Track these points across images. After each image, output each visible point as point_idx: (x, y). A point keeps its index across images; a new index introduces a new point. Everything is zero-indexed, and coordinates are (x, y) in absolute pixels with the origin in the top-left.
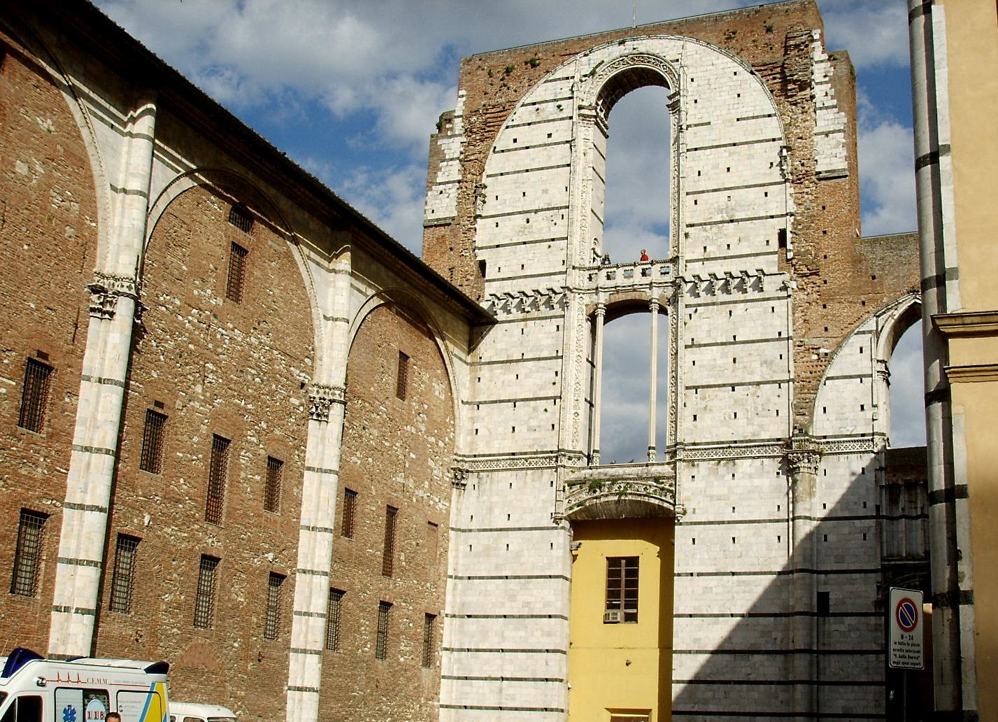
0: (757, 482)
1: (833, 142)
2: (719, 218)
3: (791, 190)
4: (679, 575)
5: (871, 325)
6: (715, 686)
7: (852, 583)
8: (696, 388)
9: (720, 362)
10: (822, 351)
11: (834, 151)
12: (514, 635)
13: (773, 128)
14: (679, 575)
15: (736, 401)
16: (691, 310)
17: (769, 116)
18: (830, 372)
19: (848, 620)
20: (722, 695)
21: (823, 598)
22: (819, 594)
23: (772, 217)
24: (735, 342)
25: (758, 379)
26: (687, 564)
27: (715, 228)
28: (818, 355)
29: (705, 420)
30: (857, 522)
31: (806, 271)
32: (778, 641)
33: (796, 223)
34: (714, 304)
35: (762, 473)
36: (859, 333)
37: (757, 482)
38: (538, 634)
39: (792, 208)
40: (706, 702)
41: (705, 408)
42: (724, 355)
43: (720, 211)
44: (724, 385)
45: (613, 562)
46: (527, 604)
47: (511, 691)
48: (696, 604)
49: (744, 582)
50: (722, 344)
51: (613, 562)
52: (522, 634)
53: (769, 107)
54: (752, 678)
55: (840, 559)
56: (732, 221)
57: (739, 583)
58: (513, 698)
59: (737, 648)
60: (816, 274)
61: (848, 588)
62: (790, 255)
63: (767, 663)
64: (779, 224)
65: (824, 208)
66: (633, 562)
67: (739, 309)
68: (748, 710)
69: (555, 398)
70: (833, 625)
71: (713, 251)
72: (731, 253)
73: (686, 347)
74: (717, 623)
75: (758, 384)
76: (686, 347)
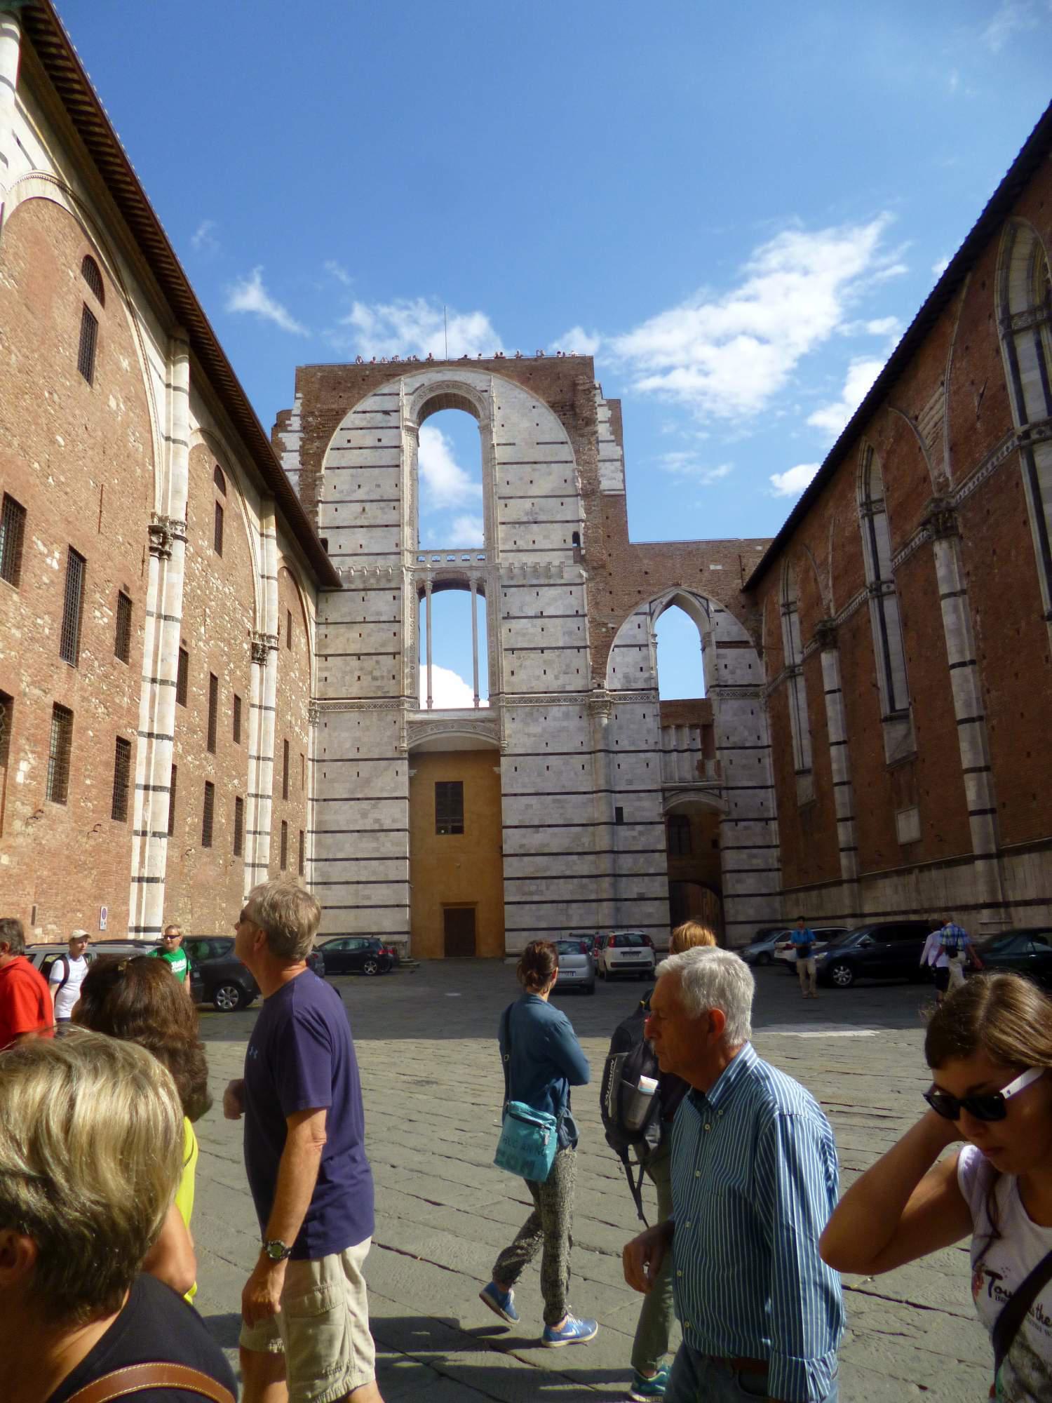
0: (565, 724)
1: (613, 468)
2: (525, 519)
3: (582, 502)
4: (505, 795)
5: (646, 608)
6: (539, 881)
7: (639, 799)
8: (513, 650)
9: (531, 630)
10: (610, 625)
11: (614, 475)
12: (367, 846)
13: (567, 452)
14: (505, 795)
15: (545, 661)
16: (505, 590)
17: (562, 443)
18: (616, 641)
19: (639, 828)
20: (544, 887)
21: (619, 811)
22: (617, 808)
23: (567, 522)
24: (541, 615)
25: (561, 644)
26: (512, 786)
27: (522, 527)
28: (607, 628)
29: (521, 675)
30: (641, 755)
31: (595, 564)
32: (587, 845)
33: (586, 527)
34: (523, 586)
35: (566, 716)
36: (636, 614)
37: (565, 724)
38: (388, 845)
39: (583, 515)
40: (531, 893)
41: (521, 666)
42: (534, 626)
43: (527, 514)
44: (535, 649)
45: (441, 787)
46: (377, 821)
47: (367, 892)
48: (520, 818)
49: (559, 801)
50: (531, 617)
51: (441, 787)
52: (375, 845)
53: (562, 435)
54: (568, 873)
55: (630, 782)
56: (536, 523)
57: (554, 801)
58: (368, 897)
59: (555, 851)
60: (603, 566)
61: (637, 804)
62: (583, 552)
63: (578, 862)
64: (571, 528)
65: (607, 518)
66: (457, 787)
67: (544, 591)
68: (565, 899)
69: (394, 654)
70: (623, 831)
71: (522, 544)
72: (536, 547)
73: (504, 618)
74: (538, 832)
75: (563, 648)
76: (504, 618)
